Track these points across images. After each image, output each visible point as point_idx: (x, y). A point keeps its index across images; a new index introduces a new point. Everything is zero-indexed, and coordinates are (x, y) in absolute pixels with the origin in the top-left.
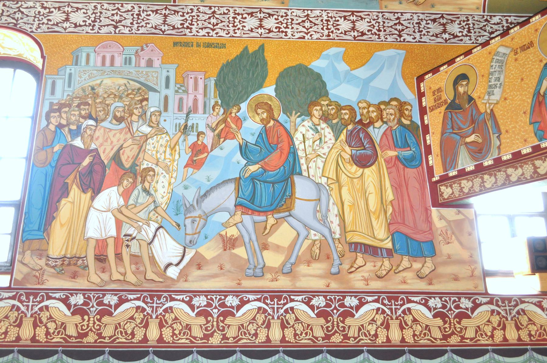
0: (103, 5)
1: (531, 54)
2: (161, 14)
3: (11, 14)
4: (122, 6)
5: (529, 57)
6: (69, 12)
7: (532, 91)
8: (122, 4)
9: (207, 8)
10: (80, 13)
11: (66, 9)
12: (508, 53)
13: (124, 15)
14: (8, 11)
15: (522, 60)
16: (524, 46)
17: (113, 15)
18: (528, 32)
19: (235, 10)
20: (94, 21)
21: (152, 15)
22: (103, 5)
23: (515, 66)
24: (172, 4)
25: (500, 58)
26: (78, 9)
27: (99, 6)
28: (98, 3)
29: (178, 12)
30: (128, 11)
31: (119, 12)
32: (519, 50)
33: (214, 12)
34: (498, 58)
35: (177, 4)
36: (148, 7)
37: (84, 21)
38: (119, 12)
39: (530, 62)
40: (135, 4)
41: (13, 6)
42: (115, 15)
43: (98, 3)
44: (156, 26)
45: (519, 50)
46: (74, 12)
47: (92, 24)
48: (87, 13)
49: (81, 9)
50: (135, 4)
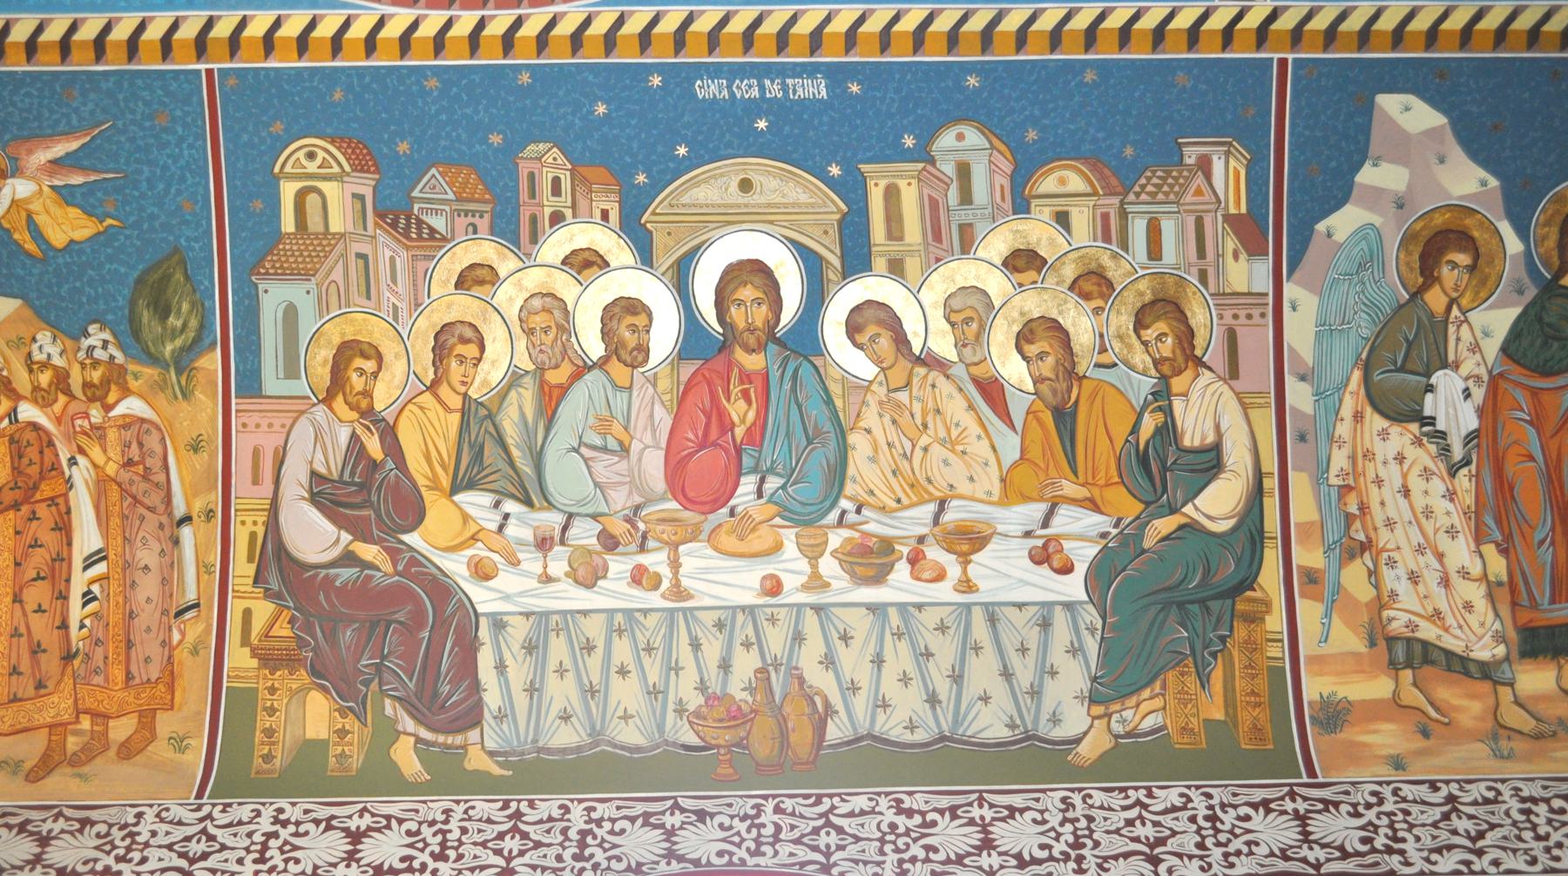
0: (1090, 796)
2: (1285, 812)
3: (803, 836)
4: (1150, 795)
6: (988, 820)
8: (1149, 789)
9: (1424, 788)
10: (711, 830)
11: (976, 812)
13: (1167, 820)
14: (793, 827)
17: (1130, 823)
19: (1517, 789)
20: (1077, 845)
21: (1258, 817)
22: (1090, 796)
24: (1305, 780)
26: (1012, 811)
27: (1077, 799)
28: (1072, 790)
29: (1336, 805)
30: (1174, 809)
31: (1144, 813)
33: (1451, 799)
35: (1321, 780)
36: (1235, 795)
37: (1042, 847)
38: (1144, 813)
40: (1189, 787)
41: (808, 812)
42: (1138, 823)
43: (1072, 790)
44: (1283, 851)
46: (1003, 820)
47: (1073, 854)
48: (1044, 822)
49: (1022, 811)
50: (1189, 787)
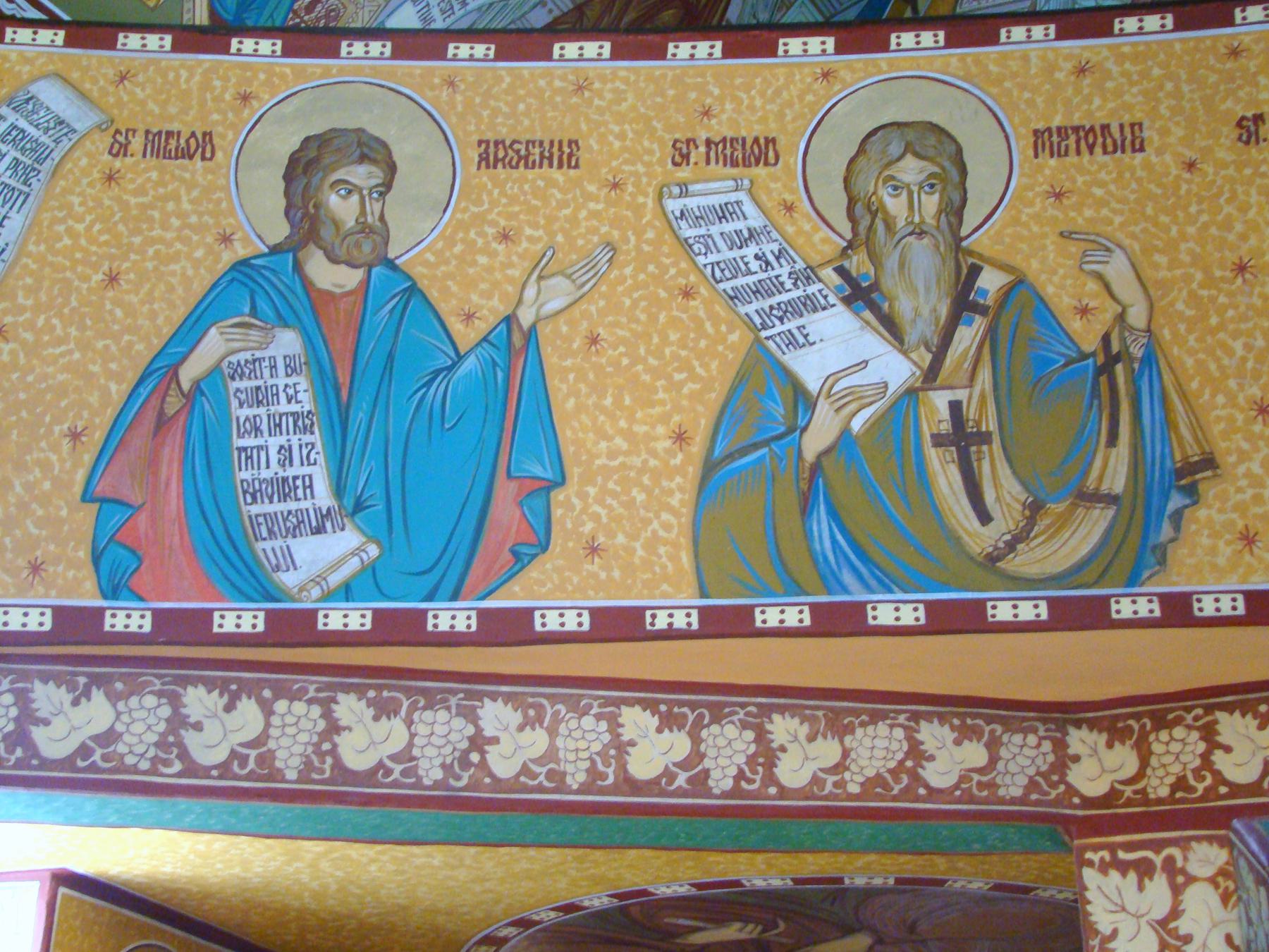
1: (191, 186)
5: (178, 199)
7: (143, 351)
12: (78, 126)
15: (140, 191)
16: (169, 134)
18: (206, 86)
23: (99, 204)
25: (31, 130)
32: (137, 143)
34: (22, 124)
39: (175, 222)
45: (137, 143)
